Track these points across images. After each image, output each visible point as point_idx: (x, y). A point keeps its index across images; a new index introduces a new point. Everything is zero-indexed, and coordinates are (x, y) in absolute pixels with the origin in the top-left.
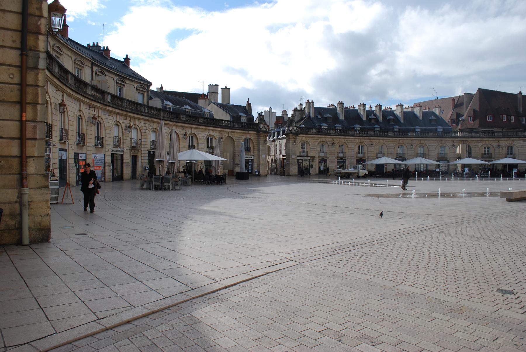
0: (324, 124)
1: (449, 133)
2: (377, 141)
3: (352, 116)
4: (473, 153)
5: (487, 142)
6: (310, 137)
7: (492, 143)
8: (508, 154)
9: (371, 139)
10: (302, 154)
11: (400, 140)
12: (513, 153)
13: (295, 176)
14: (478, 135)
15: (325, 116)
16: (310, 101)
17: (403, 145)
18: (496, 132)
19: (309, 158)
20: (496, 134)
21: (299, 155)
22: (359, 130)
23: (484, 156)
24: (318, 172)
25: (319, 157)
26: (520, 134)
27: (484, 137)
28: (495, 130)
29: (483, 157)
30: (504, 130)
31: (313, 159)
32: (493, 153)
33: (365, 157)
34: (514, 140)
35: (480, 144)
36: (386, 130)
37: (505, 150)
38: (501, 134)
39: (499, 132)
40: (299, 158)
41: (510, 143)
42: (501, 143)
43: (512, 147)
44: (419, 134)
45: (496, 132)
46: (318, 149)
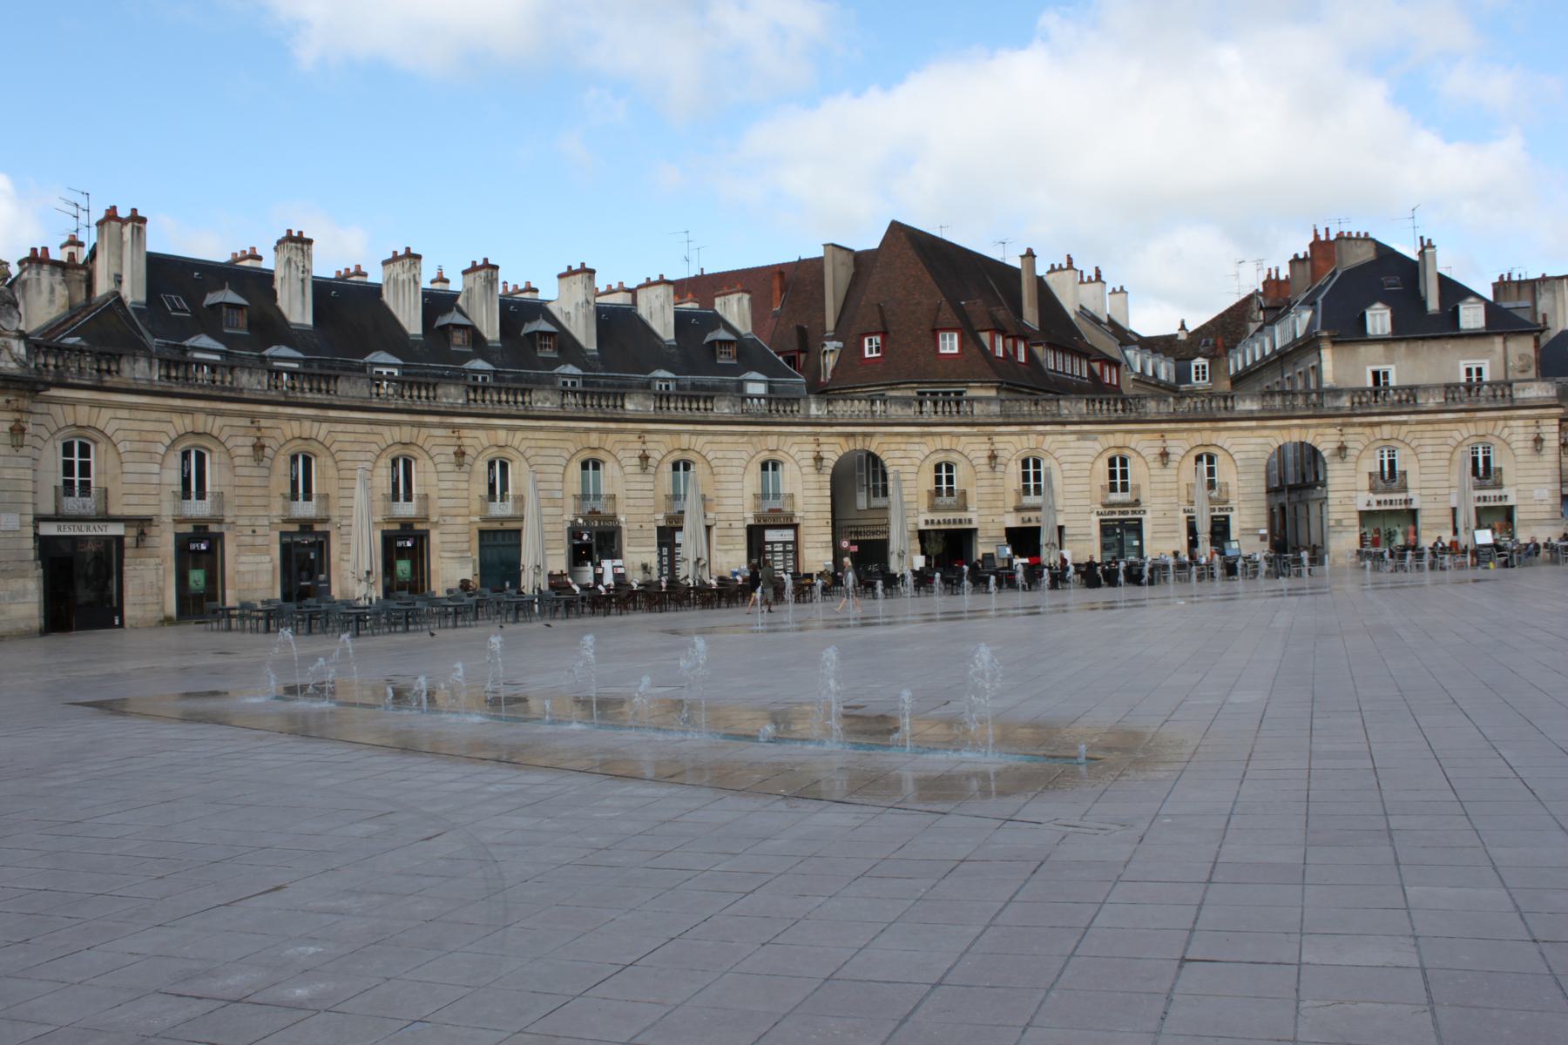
0: (204, 341)
1: (797, 400)
2: (481, 434)
3: (349, 308)
6: (122, 406)
9: (455, 427)
10: (73, 504)
13: (25, 635)
14: (910, 412)
15: (212, 299)
16: (123, 213)
17: (601, 455)
19: (115, 530)
20: (977, 408)
21: (48, 508)
22: (390, 378)
23: (938, 500)
24: (171, 608)
25: (179, 521)
27: (934, 419)
28: (970, 393)
31: (142, 535)
33: (426, 519)
36: (523, 387)
38: (995, 408)
40: (49, 529)
41: (1033, 445)
43: (1037, 464)
46: (173, 477)
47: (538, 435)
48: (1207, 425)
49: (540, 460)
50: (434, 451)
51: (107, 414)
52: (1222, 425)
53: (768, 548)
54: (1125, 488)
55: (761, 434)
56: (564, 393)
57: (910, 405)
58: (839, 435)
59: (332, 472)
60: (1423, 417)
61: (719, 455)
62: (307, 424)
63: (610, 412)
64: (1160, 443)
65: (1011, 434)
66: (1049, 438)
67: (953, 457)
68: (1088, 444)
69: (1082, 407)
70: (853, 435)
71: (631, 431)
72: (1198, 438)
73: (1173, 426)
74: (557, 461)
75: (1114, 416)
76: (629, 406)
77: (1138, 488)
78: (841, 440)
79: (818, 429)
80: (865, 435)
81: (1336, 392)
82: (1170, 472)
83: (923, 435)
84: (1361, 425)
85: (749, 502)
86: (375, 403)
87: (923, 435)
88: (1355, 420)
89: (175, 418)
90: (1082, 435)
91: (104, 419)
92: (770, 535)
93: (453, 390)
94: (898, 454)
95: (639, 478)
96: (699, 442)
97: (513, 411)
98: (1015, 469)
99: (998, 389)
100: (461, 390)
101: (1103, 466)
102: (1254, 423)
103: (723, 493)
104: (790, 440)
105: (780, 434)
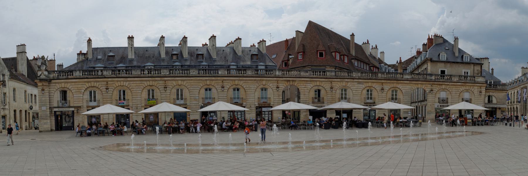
1: (272, 70)
4: (302, 96)
5: (318, 83)
6: (72, 82)
7: (325, 85)
8: (342, 98)
9: (165, 81)
11: (206, 80)
12: (347, 97)
14: (308, 74)
17: (211, 87)
18: (329, 71)
20: (328, 74)
26: (354, 75)
27: (314, 76)
28: (327, 69)
29: (313, 102)
30: (337, 70)
32: (325, 98)
34: (348, 82)
35: (310, 86)
37: (338, 95)
39: (332, 71)
42: (334, 84)
44: (233, 72)
45: (329, 71)
47: (191, 82)
48: (395, 81)
49: (192, 88)
50: (159, 87)
51: (69, 84)
52: (399, 82)
53: (263, 113)
54: (371, 98)
55: (260, 80)
56: (199, 70)
57: (307, 72)
58: (285, 81)
59: (130, 94)
60: (453, 83)
61: (248, 86)
62: (122, 82)
63: (215, 75)
64: (381, 86)
65: (338, 81)
66: (349, 83)
67: (320, 88)
68: (361, 85)
69: (359, 74)
70: (289, 81)
71: (219, 80)
72: (392, 85)
73: (385, 81)
74: (197, 88)
75: (369, 77)
76: (220, 73)
77: (375, 98)
78: (286, 82)
79: (278, 79)
80: (293, 81)
81: (431, 75)
82: (384, 94)
83: (311, 81)
84: (437, 84)
85: (256, 100)
86: (142, 75)
87: (311, 81)
88: (436, 83)
89: (87, 84)
90: (359, 83)
91: (68, 86)
92: (264, 109)
93: (165, 71)
94: (303, 86)
95: (222, 93)
96: (241, 83)
97: (183, 75)
98: (339, 92)
99: (335, 69)
100: (168, 70)
101: (365, 92)
102: (408, 82)
103: (248, 97)
104: (270, 82)
105: (266, 80)
